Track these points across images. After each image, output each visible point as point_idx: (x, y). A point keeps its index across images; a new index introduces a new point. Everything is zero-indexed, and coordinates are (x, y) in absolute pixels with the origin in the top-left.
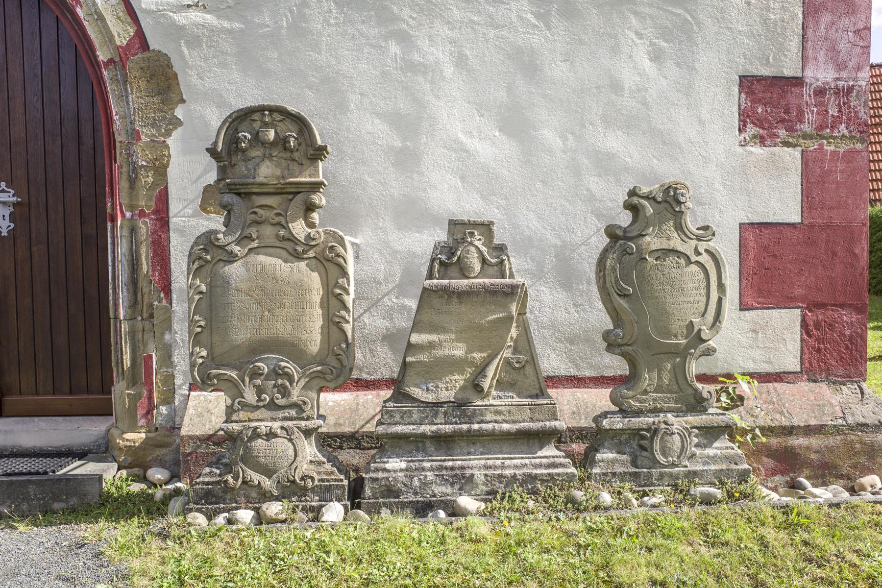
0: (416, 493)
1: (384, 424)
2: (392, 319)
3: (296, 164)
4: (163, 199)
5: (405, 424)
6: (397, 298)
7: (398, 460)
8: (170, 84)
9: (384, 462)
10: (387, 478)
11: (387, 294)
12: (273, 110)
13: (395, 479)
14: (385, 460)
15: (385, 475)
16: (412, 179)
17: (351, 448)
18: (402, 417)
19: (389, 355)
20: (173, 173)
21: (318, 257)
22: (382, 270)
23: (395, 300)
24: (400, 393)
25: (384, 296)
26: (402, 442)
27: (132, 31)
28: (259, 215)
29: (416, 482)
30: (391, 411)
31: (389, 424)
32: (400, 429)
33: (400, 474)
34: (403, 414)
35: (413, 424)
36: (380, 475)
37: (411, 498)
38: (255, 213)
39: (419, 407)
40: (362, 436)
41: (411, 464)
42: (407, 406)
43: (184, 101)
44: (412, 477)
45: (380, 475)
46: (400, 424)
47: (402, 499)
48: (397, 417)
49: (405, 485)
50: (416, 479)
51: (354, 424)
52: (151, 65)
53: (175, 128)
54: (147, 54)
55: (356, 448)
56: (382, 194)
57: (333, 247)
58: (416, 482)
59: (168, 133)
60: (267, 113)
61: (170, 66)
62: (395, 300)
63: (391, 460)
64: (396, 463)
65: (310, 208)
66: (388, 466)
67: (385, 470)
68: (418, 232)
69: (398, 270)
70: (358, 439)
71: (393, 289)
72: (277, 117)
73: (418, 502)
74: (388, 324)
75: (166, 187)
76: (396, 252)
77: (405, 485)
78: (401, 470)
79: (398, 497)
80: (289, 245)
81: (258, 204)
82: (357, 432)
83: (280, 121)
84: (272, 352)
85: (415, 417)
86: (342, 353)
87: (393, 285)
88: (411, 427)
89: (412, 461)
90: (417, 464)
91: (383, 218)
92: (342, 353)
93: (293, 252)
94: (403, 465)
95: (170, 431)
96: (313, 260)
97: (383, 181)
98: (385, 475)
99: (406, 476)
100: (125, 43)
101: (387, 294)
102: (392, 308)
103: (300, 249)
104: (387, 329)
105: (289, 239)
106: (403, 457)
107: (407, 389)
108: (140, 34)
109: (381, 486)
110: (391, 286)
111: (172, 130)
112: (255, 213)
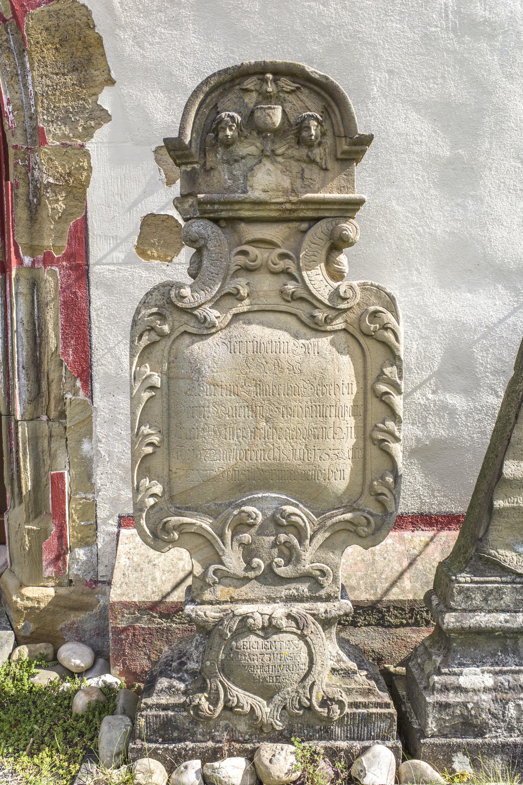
0: (510, 729)
1: (455, 610)
2: (425, 424)
3: (315, 169)
4: (81, 234)
5: (490, 612)
6: (434, 392)
7: (478, 670)
8: (91, 55)
9: (455, 674)
10: (465, 705)
11: (419, 387)
12: (280, 71)
13: (477, 705)
14: (456, 670)
15: (460, 698)
16: (465, 208)
17: (369, 625)
18: (485, 600)
19: (419, 478)
20: (94, 195)
21: (351, 329)
22: (414, 350)
23: (430, 396)
24: (481, 558)
25: (414, 390)
26: (481, 638)
28: (252, 256)
29: (512, 711)
30: (468, 589)
31: (464, 610)
32: (482, 619)
33: (485, 697)
34: (487, 595)
35: (503, 611)
36: (452, 698)
37: (503, 737)
38: (244, 253)
39: (513, 582)
40: (388, 607)
41: (501, 678)
42: (493, 581)
43: (111, 82)
44: (505, 703)
45: (452, 698)
46: (481, 610)
47: (489, 738)
48: (478, 600)
49: (494, 716)
50: (511, 705)
51: (373, 587)
52: (62, 24)
53: (99, 125)
55: (377, 625)
56: (417, 232)
57: (376, 312)
58: (512, 711)
59: (88, 133)
60: (270, 76)
61: (90, 25)
62: (430, 396)
63: (466, 670)
64: (475, 678)
65: (337, 244)
66: (463, 681)
67: (459, 689)
68: (470, 291)
69: (437, 351)
70: (380, 612)
71: (429, 378)
72: (287, 84)
73: (515, 745)
74: (419, 433)
75: (85, 219)
76: (436, 322)
77: (494, 716)
78: (486, 690)
79: (482, 735)
80: (302, 309)
81: (250, 237)
82: (379, 601)
84: (270, 488)
85: (507, 599)
86: (386, 491)
87: (429, 372)
88: (502, 617)
89: (501, 672)
90: (509, 677)
91: (417, 270)
92: (386, 491)
94: (489, 681)
95: (90, 586)
96: (342, 335)
97: (419, 211)
98: (460, 698)
99: (495, 700)
101: (419, 387)
102: (426, 408)
103: (320, 315)
104: (418, 440)
105: (302, 299)
106: (484, 664)
107: (492, 551)
109: (453, 716)
110: (425, 375)
111: (94, 128)
112: (244, 253)
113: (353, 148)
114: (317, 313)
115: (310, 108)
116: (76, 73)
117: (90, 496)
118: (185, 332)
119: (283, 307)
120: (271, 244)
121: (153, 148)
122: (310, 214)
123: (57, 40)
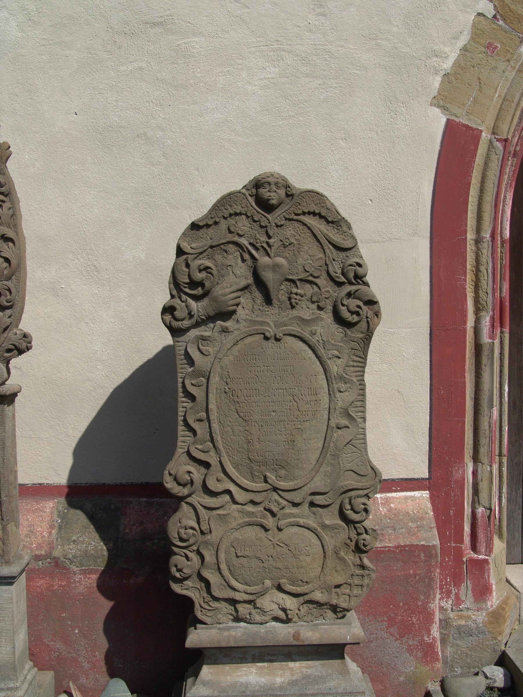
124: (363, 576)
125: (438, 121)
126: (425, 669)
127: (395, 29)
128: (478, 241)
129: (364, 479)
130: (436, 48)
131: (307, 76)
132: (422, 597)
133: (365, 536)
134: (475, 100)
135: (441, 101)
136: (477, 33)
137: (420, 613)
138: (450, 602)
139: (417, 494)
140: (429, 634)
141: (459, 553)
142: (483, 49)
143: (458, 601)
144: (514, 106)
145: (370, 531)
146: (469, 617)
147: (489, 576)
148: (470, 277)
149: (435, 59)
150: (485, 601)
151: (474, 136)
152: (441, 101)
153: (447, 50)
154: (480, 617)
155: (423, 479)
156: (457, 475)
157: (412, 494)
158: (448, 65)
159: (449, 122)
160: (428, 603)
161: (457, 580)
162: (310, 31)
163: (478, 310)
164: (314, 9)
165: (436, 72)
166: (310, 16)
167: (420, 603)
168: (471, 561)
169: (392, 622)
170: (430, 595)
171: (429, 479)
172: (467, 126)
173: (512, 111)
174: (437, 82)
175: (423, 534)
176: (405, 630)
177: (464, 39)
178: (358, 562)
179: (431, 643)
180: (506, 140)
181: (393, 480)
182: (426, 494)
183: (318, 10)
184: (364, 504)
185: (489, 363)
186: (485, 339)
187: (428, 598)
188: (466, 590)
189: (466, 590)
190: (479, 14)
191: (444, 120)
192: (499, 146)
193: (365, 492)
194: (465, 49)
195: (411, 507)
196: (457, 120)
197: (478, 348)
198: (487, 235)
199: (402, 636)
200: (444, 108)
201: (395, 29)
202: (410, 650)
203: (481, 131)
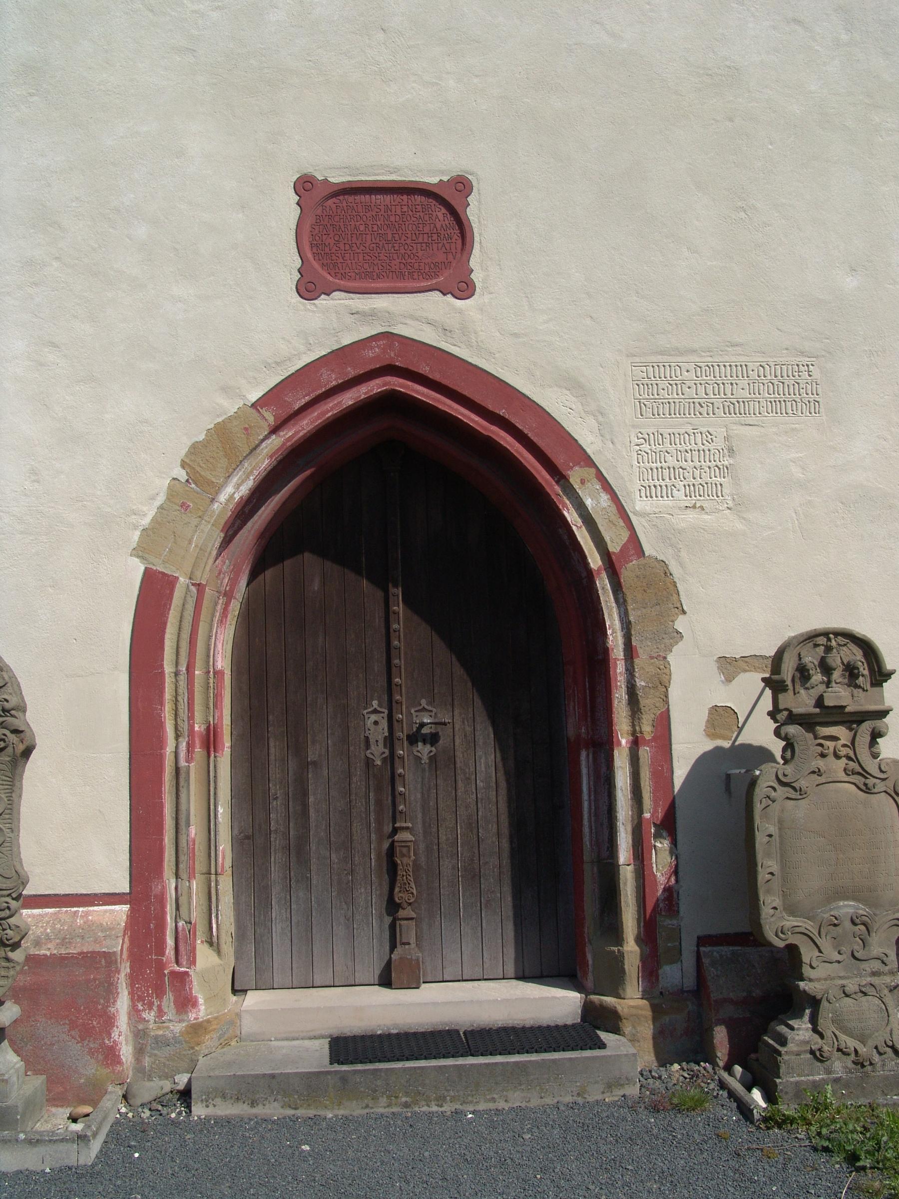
3: (860, 690)
12: (838, 633)
21: (889, 791)
27: (625, 535)
28: (826, 747)
38: (821, 745)
43: (684, 612)
53: (677, 643)
54: (642, 561)
60: (831, 636)
61: (667, 573)
65: (876, 735)
72: (841, 640)
75: (668, 710)
81: (822, 735)
83: (845, 645)
93: (864, 788)
96: (883, 794)
100: (618, 549)
105: (859, 774)
108: (634, 539)
112: (821, 745)
113: (880, 676)
114: (867, 781)
115: (856, 655)
116: (658, 607)
117: (675, 922)
118: (787, 798)
119: (847, 779)
120: (834, 738)
121: (715, 658)
122: (859, 719)
123: (644, 584)
124: (8, 968)
125: (137, 569)
126: (105, 1071)
127: (99, 493)
128: (177, 674)
129: (8, 881)
130: (134, 507)
131: (22, 533)
132: (102, 1001)
133: (8, 931)
134: (171, 551)
135: (140, 551)
136: (172, 493)
137: (100, 1016)
138: (153, 1014)
139: (117, 907)
140: (110, 1038)
141: (160, 966)
142: (178, 508)
143: (161, 1012)
144: (206, 554)
145: (13, 927)
146: (168, 1027)
147: (191, 989)
148: (168, 708)
149: (134, 517)
150: (186, 1013)
151: (170, 582)
152: (140, 551)
153: (145, 509)
154: (178, 1028)
155: (124, 894)
156: (156, 889)
157: (113, 907)
158: (146, 521)
159: (147, 572)
160: (108, 1006)
161: (160, 992)
162: (26, 495)
163: (177, 737)
164: (29, 477)
165: (135, 527)
166: (27, 483)
167: (100, 1007)
168: (173, 973)
169: (73, 1025)
170: (109, 999)
171: (129, 893)
172: (163, 574)
173: (205, 560)
174: (136, 535)
175: (108, 942)
176: (86, 1033)
177: (161, 499)
178: (4, 955)
179: (112, 1046)
180: (199, 585)
181: (96, 895)
182: (126, 908)
183: (33, 478)
184: (7, 903)
185: (186, 785)
186: (183, 763)
187: (108, 1002)
188: (168, 1001)
189: (168, 1001)
190: (174, 479)
191: (142, 568)
192: (194, 589)
193: (9, 892)
194: (161, 508)
195: (106, 920)
196: (155, 568)
197: (177, 770)
198: (183, 669)
199: (83, 1039)
200: (142, 558)
201: (99, 493)
202: (91, 1053)
203: (177, 578)
